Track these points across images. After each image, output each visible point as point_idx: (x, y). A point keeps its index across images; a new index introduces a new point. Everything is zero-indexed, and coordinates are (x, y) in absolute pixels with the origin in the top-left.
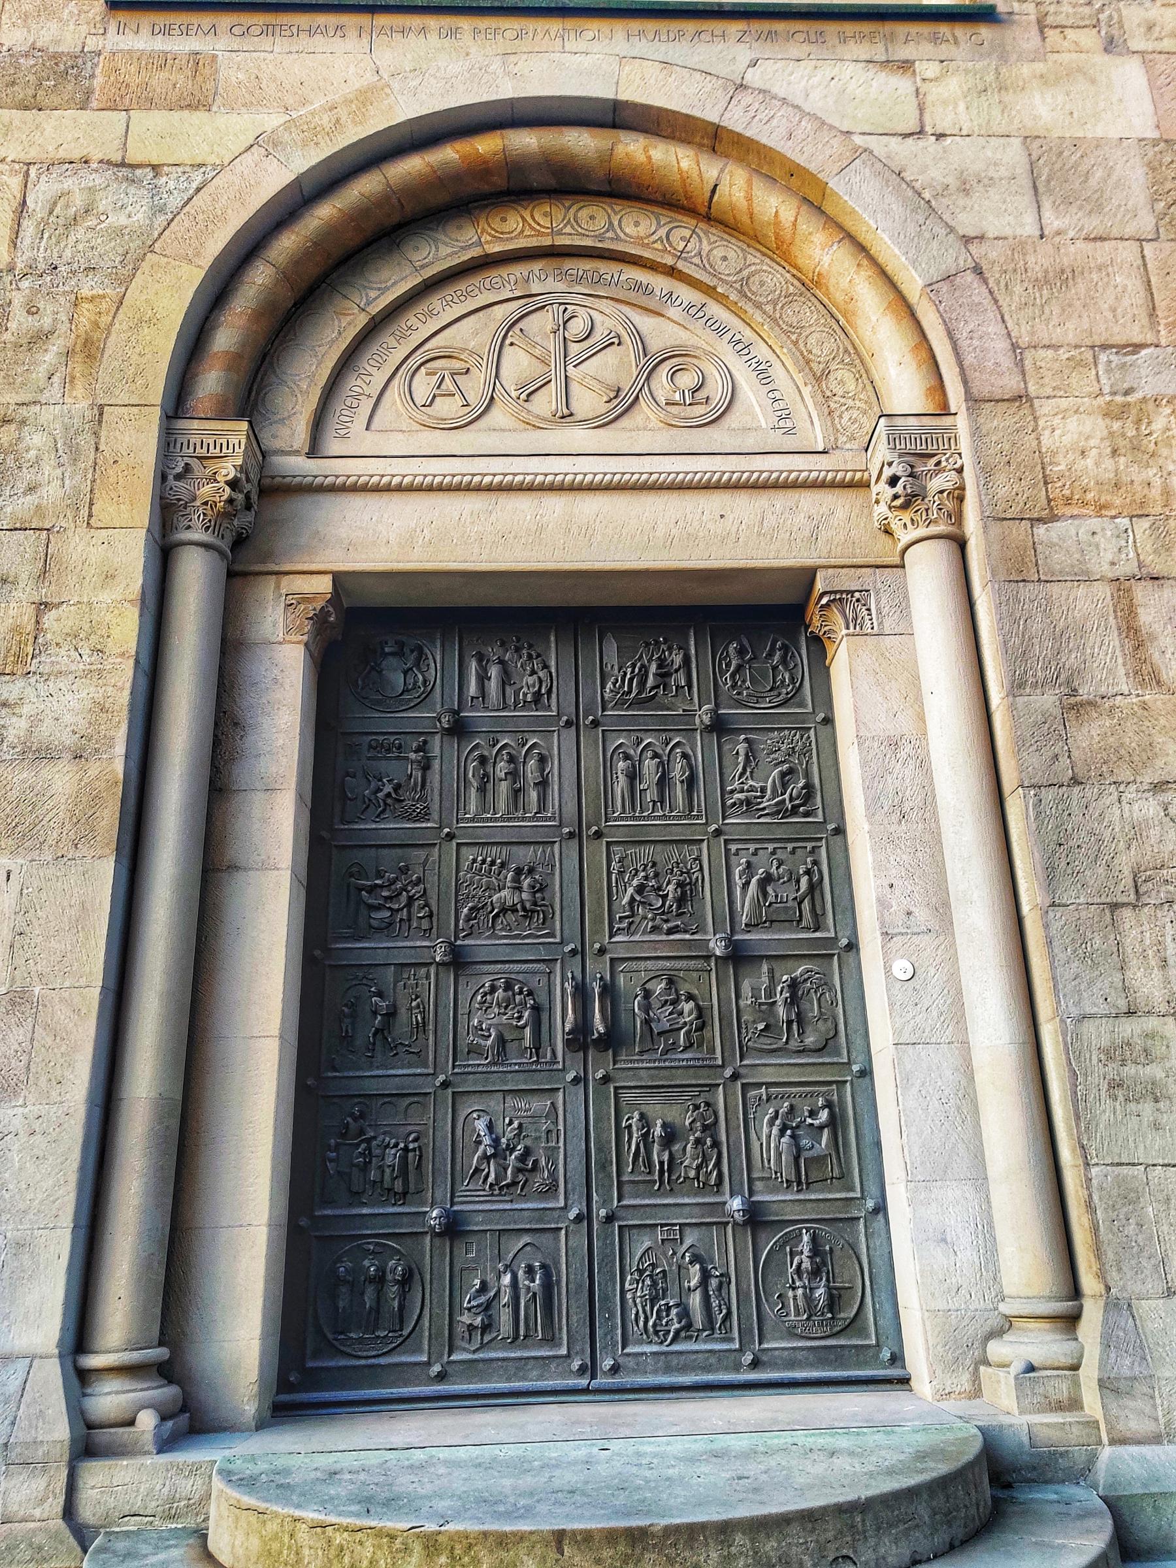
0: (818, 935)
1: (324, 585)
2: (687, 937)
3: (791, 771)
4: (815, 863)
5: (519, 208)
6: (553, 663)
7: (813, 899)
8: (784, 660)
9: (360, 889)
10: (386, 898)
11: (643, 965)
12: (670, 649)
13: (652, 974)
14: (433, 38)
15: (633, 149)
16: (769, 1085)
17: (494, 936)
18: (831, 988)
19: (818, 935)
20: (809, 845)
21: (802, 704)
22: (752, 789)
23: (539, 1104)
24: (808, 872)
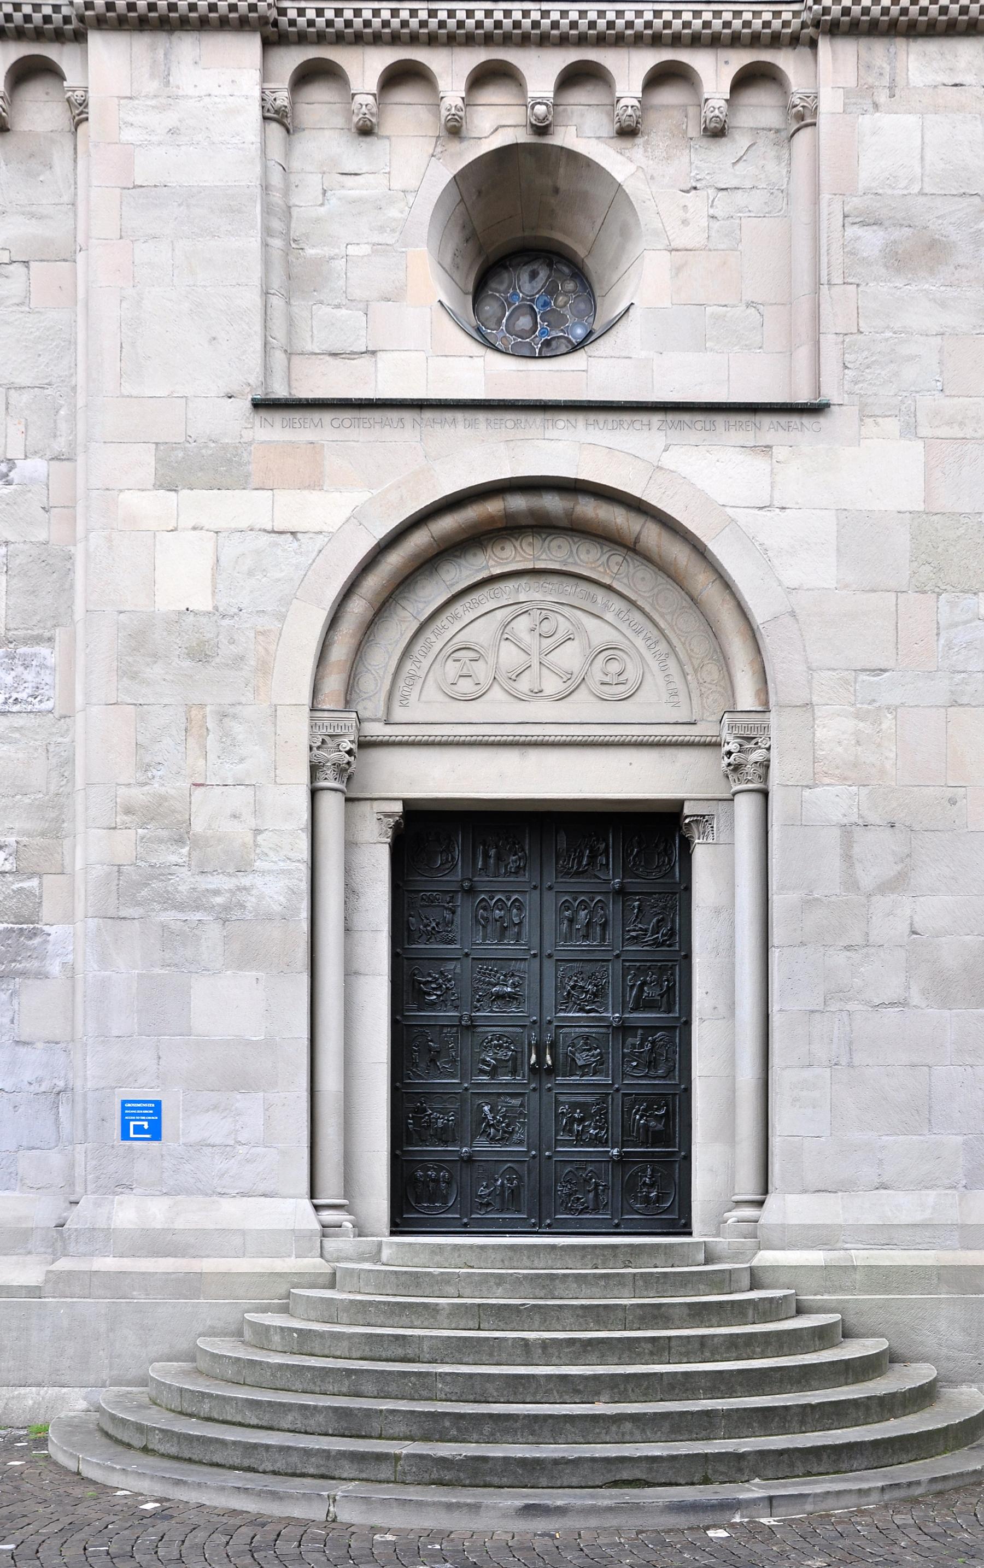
0: (671, 1015)
1: (398, 807)
2: (598, 1015)
3: (663, 919)
4: (672, 974)
5: (513, 540)
6: (527, 847)
7: (669, 996)
8: (665, 850)
9: (420, 982)
10: (434, 989)
11: (573, 1030)
12: (598, 840)
13: (577, 1035)
14: (460, 426)
15: (589, 509)
16: (636, 1094)
17: (492, 1011)
18: (674, 1044)
19: (671, 1015)
20: (670, 964)
21: (674, 877)
22: (641, 929)
23: (516, 1102)
24: (667, 980)
